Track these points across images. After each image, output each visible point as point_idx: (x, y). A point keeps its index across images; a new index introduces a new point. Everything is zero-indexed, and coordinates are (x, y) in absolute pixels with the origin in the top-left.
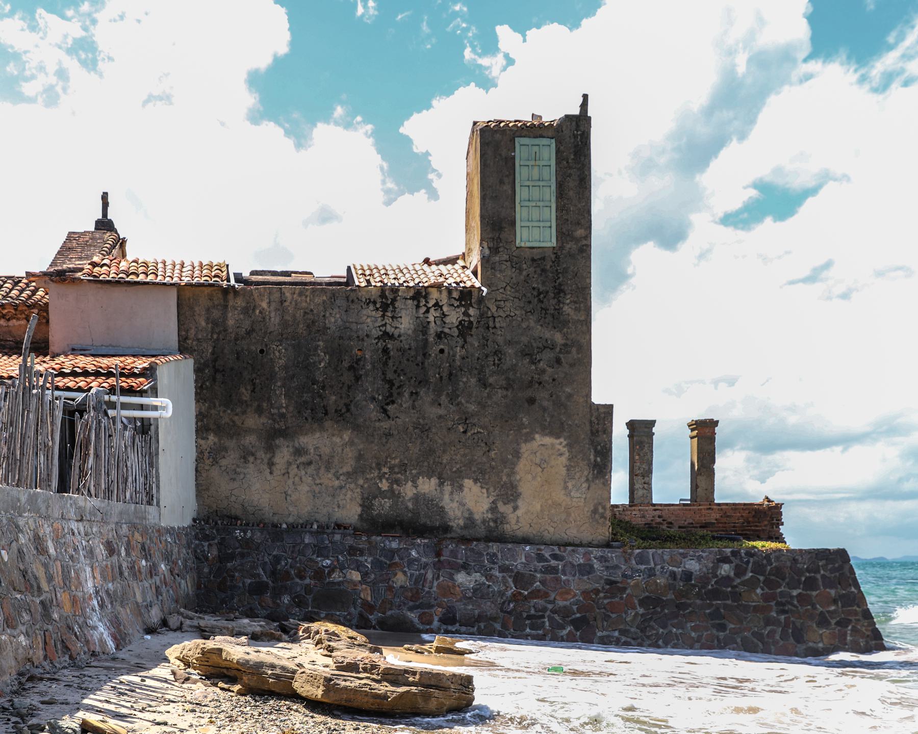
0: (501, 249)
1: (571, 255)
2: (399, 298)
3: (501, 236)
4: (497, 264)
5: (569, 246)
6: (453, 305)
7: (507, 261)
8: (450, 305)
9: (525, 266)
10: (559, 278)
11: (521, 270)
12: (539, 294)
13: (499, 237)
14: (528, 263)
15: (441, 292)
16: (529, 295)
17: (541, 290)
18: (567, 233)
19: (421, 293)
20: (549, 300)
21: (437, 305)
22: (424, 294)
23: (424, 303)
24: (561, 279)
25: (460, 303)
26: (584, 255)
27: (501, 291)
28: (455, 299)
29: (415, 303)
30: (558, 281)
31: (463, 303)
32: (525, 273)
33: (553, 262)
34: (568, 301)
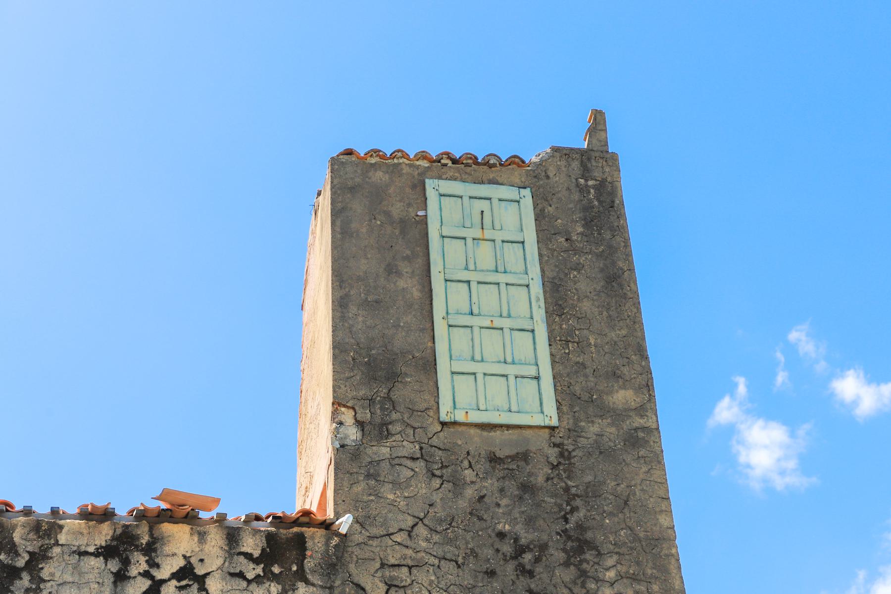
0: (394, 428)
1: (602, 451)
2: (57, 550)
3: (395, 395)
4: (385, 465)
5: (594, 429)
6: (241, 575)
7: (413, 459)
8: (232, 575)
9: (469, 474)
10: (574, 510)
11: (458, 484)
12: (520, 551)
13: (388, 398)
14: (477, 467)
15: (202, 536)
16: (489, 552)
17: (523, 541)
18: (585, 396)
19: (138, 537)
20: (550, 569)
21: (186, 573)
22: (145, 540)
23: (144, 567)
24: (582, 514)
25: (267, 571)
26: (642, 453)
27: (398, 538)
28: (248, 556)
29: (114, 565)
30: (573, 519)
31: (276, 569)
32: (469, 492)
33: (554, 467)
34: (611, 574)
